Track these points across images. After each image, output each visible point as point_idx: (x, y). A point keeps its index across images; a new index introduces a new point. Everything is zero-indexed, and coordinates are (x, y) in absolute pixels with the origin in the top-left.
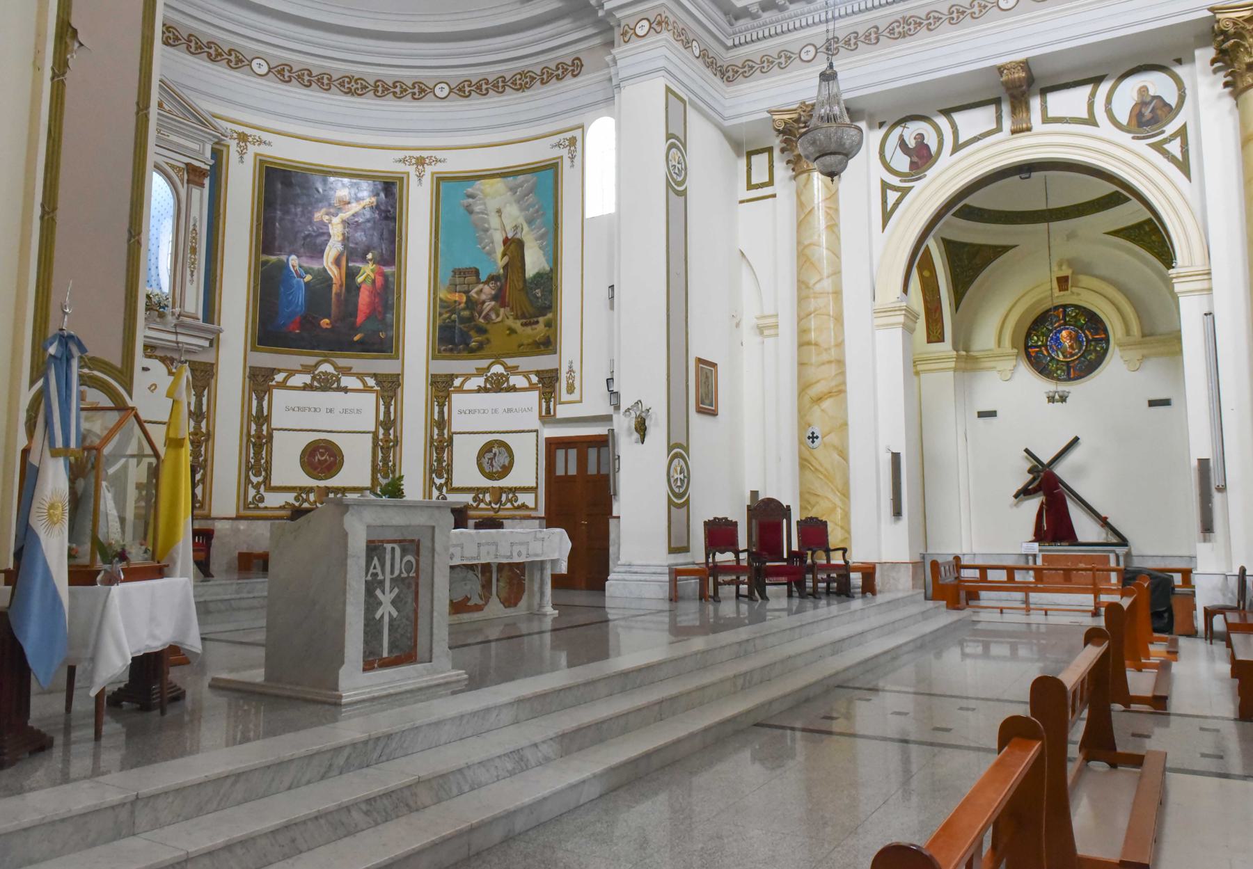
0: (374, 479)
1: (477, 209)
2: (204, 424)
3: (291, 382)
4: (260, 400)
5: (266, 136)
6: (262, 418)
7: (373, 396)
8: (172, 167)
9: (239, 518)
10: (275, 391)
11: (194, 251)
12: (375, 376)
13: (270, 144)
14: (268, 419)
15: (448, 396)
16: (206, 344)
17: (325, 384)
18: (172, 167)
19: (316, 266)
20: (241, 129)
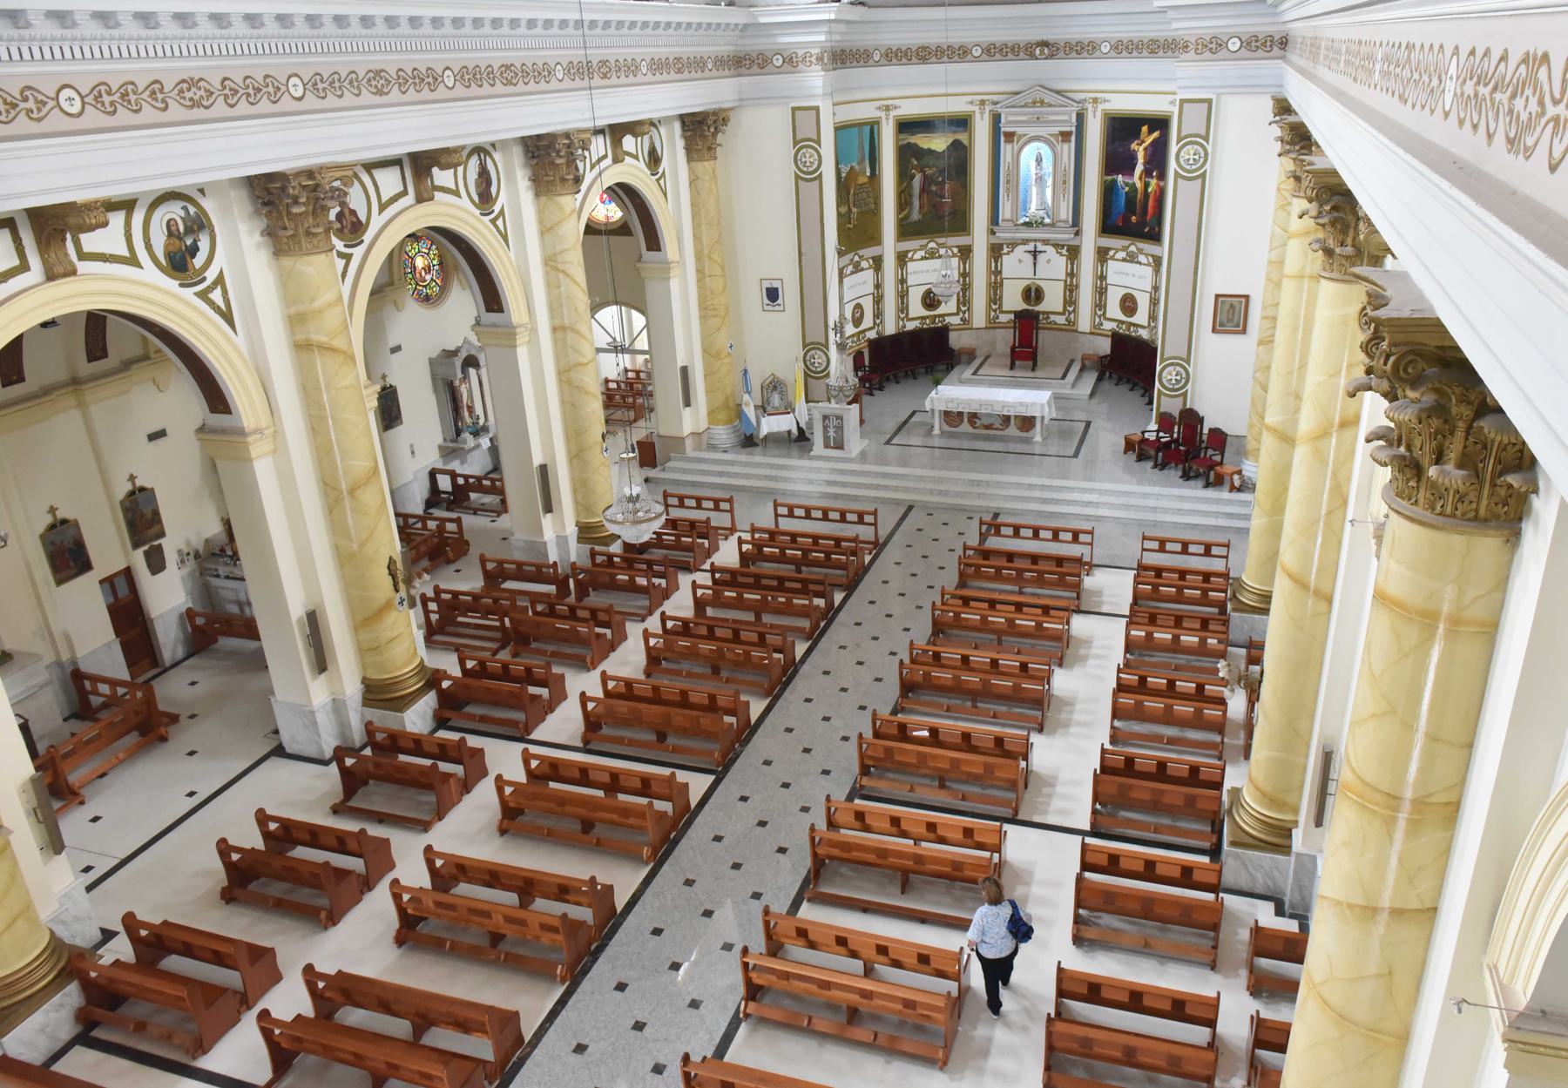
3: (1117, 256)
4: (1102, 266)
5: (1107, 96)
6: (1103, 277)
7: (1151, 269)
8: (1052, 135)
9: (1091, 333)
10: (1109, 262)
11: (1064, 182)
12: (1153, 256)
16: (1072, 236)
17: (1131, 259)
19: (1130, 182)
20: (1093, 95)
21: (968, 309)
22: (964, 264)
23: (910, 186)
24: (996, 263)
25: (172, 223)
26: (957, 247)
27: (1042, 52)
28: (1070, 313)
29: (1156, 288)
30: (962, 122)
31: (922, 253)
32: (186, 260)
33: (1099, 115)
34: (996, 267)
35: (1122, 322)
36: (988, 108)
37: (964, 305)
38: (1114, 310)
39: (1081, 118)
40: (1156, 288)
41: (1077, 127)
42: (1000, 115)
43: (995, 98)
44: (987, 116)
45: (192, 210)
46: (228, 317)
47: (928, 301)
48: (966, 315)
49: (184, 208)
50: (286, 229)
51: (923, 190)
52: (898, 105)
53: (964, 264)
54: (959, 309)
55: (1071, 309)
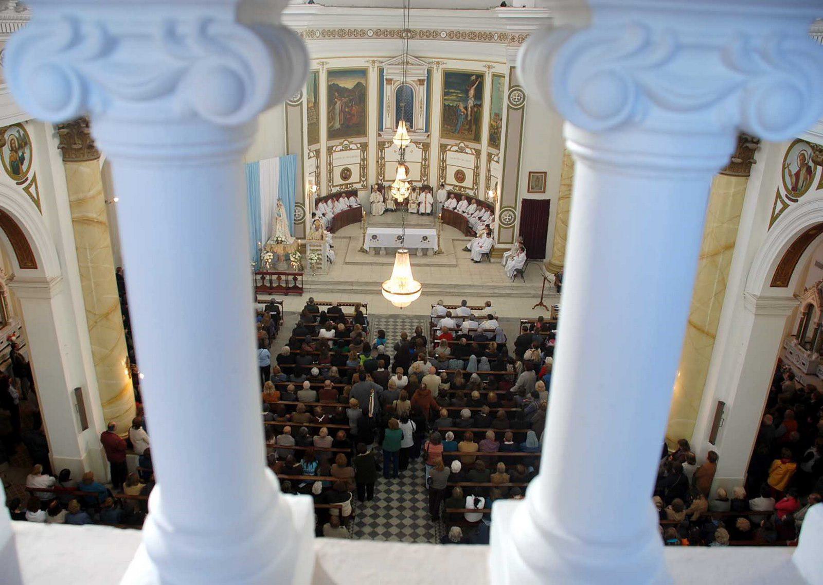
0: (473, 186)
1: (501, 89)
2: (427, 162)
3: (452, 149)
4: (443, 155)
5: (445, 61)
6: (444, 161)
7: (474, 156)
8: (414, 81)
12: (475, 149)
13: (446, 64)
14: (445, 161)
15: (491, 161)
17: (461, 150)
18: (414, 81)
20: (436, 60)
21: (366, 180)
22: (364, 153)
23: (334, 108)
24: (381, 152)
25: (13, 141)
26: (360, 143)
27: (407, 35)
28: (424, 181)
29: (477, 167)
30: (363, 72)
31: (340, 147)
32: (19, 167)
33: (440, 71)
34: (382, 155)
35: (457, 186)
36: (377, 64)
37: (364, 177)
38: (451, 179)
39: (429, 72)
40: (477, 167)
41: (427, 77)
42: (383, 69)
43: (380, 59)
44: (376, 69)
45: (22, 132)
46: (37, 202)
47: (344, 175)
48: (365, 183)
49: (18, 131)
50: (75, 144)
51: (341, 111)
52: (329, 61)
53: (364, 153)
54: (360, 179)
55: (425, 179)
